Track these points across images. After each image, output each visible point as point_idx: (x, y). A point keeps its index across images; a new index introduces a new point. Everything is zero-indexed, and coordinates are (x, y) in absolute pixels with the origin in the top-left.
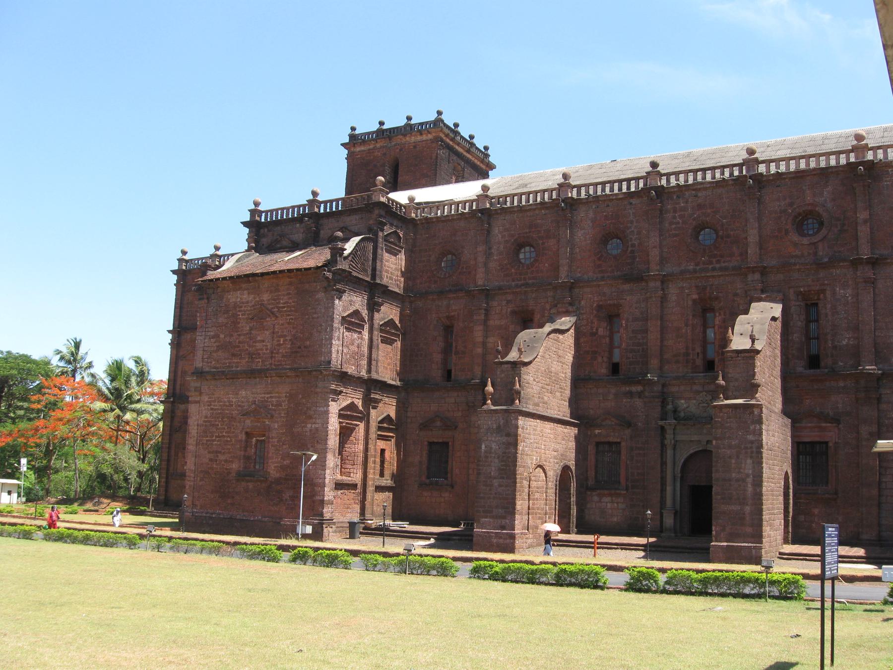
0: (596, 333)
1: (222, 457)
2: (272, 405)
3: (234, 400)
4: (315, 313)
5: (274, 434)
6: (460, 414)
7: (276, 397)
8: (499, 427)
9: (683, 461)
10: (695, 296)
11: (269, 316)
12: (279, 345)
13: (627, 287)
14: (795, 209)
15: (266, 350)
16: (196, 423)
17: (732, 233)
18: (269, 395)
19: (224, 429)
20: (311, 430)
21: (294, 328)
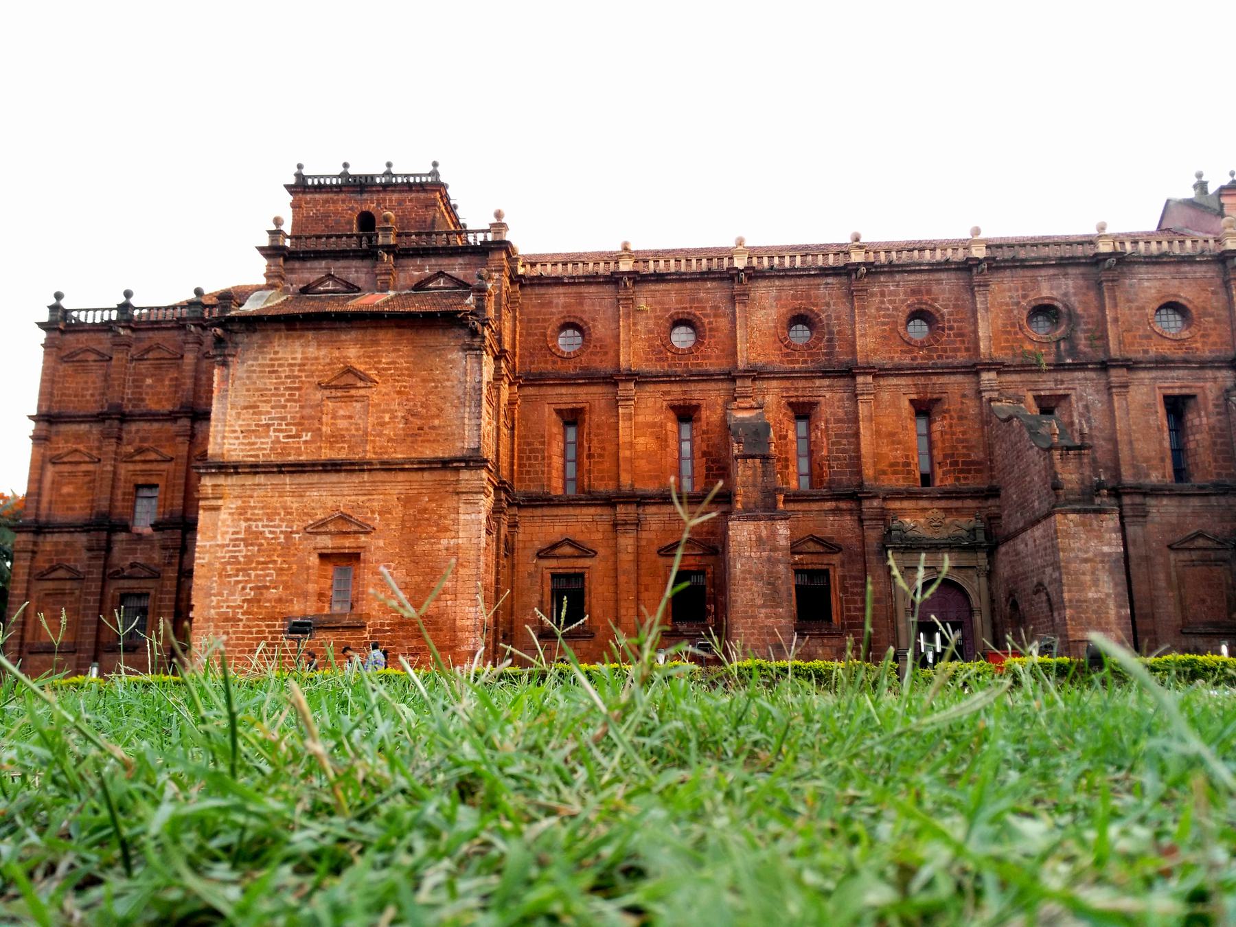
2: (373, 512)
3: (295, 505)
6: (600, 536)
7: (379, 500)
8: (760, 540)
10: (914, 397)
12: (383, 424)
13: (827, 382)
17: (955, 325)
18: (365, 498)
20: (447, 549)
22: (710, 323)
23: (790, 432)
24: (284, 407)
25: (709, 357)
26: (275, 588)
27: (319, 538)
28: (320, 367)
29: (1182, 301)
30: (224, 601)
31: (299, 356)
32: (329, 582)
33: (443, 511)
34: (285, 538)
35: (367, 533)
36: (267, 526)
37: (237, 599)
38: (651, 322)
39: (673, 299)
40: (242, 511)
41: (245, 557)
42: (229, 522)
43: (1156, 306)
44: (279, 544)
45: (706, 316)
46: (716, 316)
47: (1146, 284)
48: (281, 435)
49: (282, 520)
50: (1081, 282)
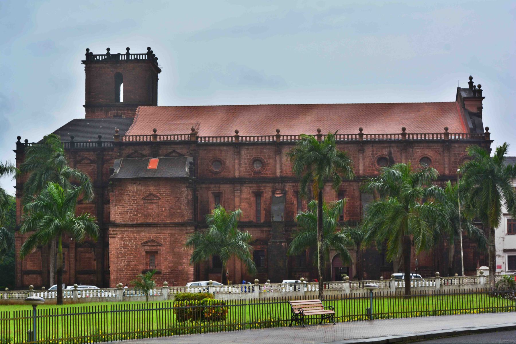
0: (293, 203)
1: (133, 263)
2: (161, 239)
3: (138, 237)
4: (182, 197)
7: (163, 235)
9: (332, 258)
11: (155, 197)
12: (162, 211)
14: (378, 156)
15: (155, 213)
16: (114, 247)
18: (157, 235)
19: (133, 250)
21: (170, 204)
23: (295, 201)
25: (267, 174)
26: (133, 261)
27: (145, 247)
28: (142, 193)
29: (429, 157)
30: (119, 265)
31: (135, 189)
32: (149, 260)
33: (182, 239)
34: (135, 247)
35: (160, 246)
36: (130, 243)
37: (123, 264)
38: (246, 161)
39: (254, 153)
40: (122, 238)
41: (124, 252)
42: (118, 242)
43: (420, 158)
44: (134, 248)
46: (269, 159)
47: (417, 150)
48: (132, 215)
49: (134, 241)
50: (395, 149)
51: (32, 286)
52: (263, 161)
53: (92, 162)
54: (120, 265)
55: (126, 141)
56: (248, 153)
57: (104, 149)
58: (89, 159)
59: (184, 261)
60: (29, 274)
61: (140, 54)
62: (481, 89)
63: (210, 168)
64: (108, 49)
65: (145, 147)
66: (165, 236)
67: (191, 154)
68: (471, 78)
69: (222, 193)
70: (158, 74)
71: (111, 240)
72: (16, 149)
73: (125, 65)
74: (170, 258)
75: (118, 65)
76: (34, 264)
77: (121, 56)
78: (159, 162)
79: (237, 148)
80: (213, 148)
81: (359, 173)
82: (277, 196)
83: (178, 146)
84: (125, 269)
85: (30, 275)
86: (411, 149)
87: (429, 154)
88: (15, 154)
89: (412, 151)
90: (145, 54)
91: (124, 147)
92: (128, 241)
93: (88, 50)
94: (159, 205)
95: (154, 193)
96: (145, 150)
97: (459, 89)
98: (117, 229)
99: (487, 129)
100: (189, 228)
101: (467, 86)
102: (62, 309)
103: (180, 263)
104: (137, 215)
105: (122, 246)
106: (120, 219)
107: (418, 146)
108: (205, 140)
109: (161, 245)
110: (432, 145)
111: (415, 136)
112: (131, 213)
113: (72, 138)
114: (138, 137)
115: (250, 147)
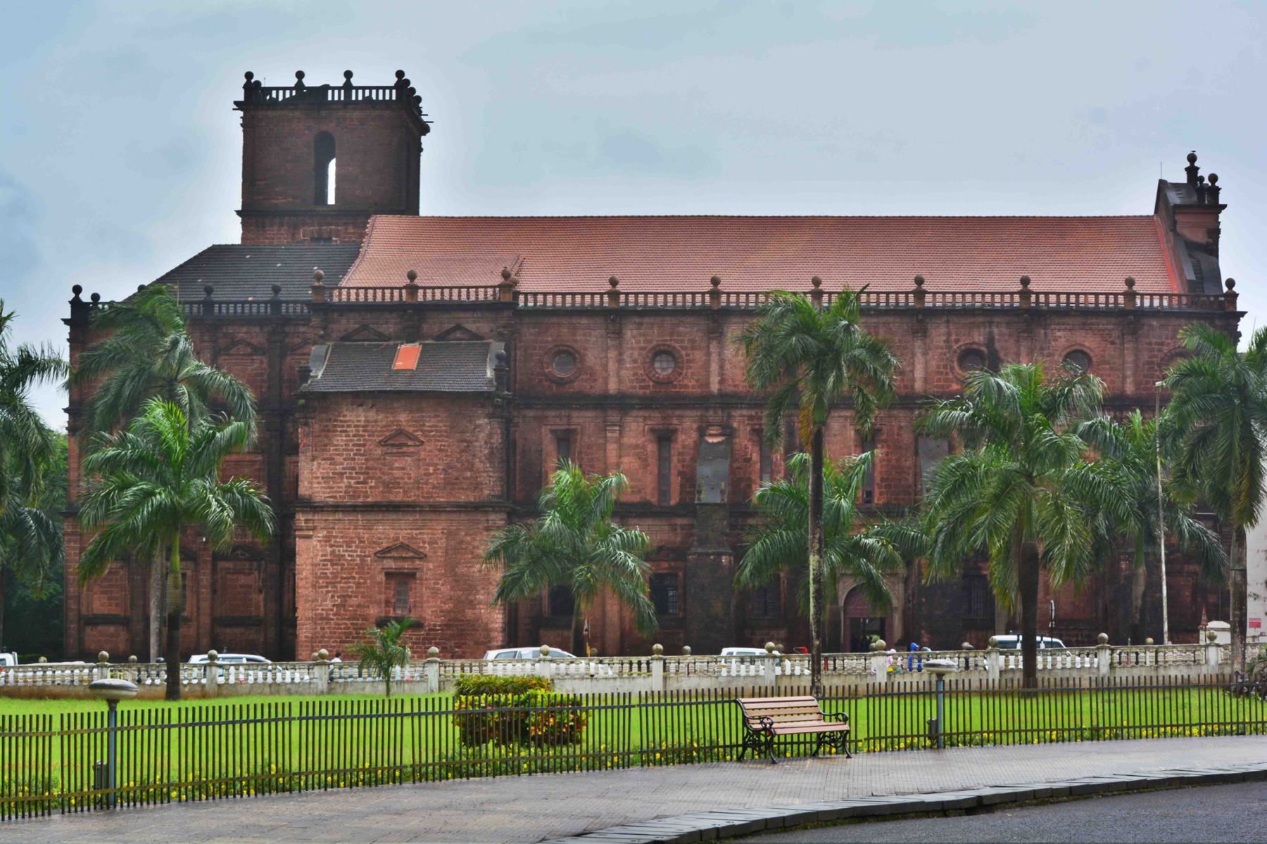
0: (751, 459)
2: (424, 542)
3: (366, 536)
5: (429, 575)
7: (428, 534)
11: (410, 439)
15: (410, 478)
16: (309, 562)
18: (417, 532)
22: (687, 355)
23: (754, 455)
24: (354, 459)
25: (686, 386)
27: (385, 561)
29: (1085, 349)
31: (363, 419)
32: (392, 593)
33: (476, 543)
35: (420, 559)
37: (329, 604)
38: (636, 353)
39: (655, 334)
40: (327, 539)
41: (332, 573)
42: (318, 547)
43: (1064, 353)
45: (684, 348)
46: (693, 348)
47: (1058, 334)
48: (353, 481)
50: (1004, 330)
51: (105, 653)
52: (677, 355)
53: (256, 350)
54: (321, 605)
55: (340, 300)
56: (640, 335)
57: (287, 321)
58: (249, 344)
59: (480, 597)
60: (97, 624)
61: (377, 88)
62: (1217, 184)
63: (547, 371)
64: (300, 75)
65: (387, 315)
66: (433, 534)
67: (500, 334)
68: (1192, 158)
69: (575, 430)
70: (423, 137)
71: (300, 545)
72: (68, 316)
73: (341, 113)
74: (445, 589)
75: (324, 113)
76: (109, 599)
77: (330, 92)
78: (422, 352)
79: (613, 321)
80: (555, 320)
81: (912, 387)
82: (710, 440)
83: (468, 315)
84: (334, 615)
85: (100, 628)
86: (1042, 331)
87: (1087, 344)
88: (67, 329)
89: (1046, 334)
90: (390, 88)
91: (336, 315)
92: (341, 546)
93: (249, 75)
94: (419, 460)
95: (407, 429)
96: (386, 323)
97: (1162, 184)
98: (316, 518)
99: (1231, 283)
100: (492, 517)
101: (1182, 178)
102: (180, 709)
103: (471, 602)
104: (365, 482)
105: (329, 557)
106: (324, 493)
107: (1058, 324)
108: (535, 302)
109: (423, 557)
110: (1094, 321)
111: (1053, 298)
112: (352, 478)
113: (209, 291)
114: (370, 292)
115: (646, 320)
